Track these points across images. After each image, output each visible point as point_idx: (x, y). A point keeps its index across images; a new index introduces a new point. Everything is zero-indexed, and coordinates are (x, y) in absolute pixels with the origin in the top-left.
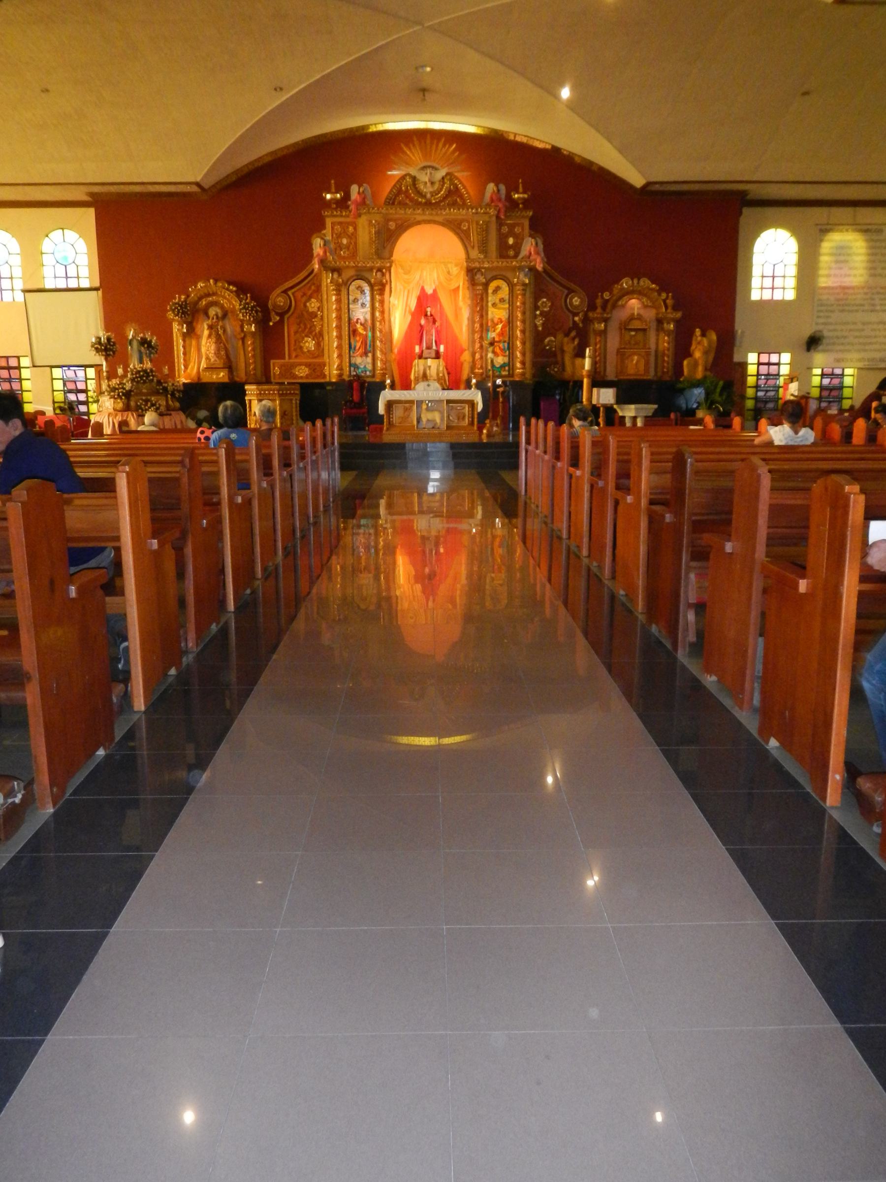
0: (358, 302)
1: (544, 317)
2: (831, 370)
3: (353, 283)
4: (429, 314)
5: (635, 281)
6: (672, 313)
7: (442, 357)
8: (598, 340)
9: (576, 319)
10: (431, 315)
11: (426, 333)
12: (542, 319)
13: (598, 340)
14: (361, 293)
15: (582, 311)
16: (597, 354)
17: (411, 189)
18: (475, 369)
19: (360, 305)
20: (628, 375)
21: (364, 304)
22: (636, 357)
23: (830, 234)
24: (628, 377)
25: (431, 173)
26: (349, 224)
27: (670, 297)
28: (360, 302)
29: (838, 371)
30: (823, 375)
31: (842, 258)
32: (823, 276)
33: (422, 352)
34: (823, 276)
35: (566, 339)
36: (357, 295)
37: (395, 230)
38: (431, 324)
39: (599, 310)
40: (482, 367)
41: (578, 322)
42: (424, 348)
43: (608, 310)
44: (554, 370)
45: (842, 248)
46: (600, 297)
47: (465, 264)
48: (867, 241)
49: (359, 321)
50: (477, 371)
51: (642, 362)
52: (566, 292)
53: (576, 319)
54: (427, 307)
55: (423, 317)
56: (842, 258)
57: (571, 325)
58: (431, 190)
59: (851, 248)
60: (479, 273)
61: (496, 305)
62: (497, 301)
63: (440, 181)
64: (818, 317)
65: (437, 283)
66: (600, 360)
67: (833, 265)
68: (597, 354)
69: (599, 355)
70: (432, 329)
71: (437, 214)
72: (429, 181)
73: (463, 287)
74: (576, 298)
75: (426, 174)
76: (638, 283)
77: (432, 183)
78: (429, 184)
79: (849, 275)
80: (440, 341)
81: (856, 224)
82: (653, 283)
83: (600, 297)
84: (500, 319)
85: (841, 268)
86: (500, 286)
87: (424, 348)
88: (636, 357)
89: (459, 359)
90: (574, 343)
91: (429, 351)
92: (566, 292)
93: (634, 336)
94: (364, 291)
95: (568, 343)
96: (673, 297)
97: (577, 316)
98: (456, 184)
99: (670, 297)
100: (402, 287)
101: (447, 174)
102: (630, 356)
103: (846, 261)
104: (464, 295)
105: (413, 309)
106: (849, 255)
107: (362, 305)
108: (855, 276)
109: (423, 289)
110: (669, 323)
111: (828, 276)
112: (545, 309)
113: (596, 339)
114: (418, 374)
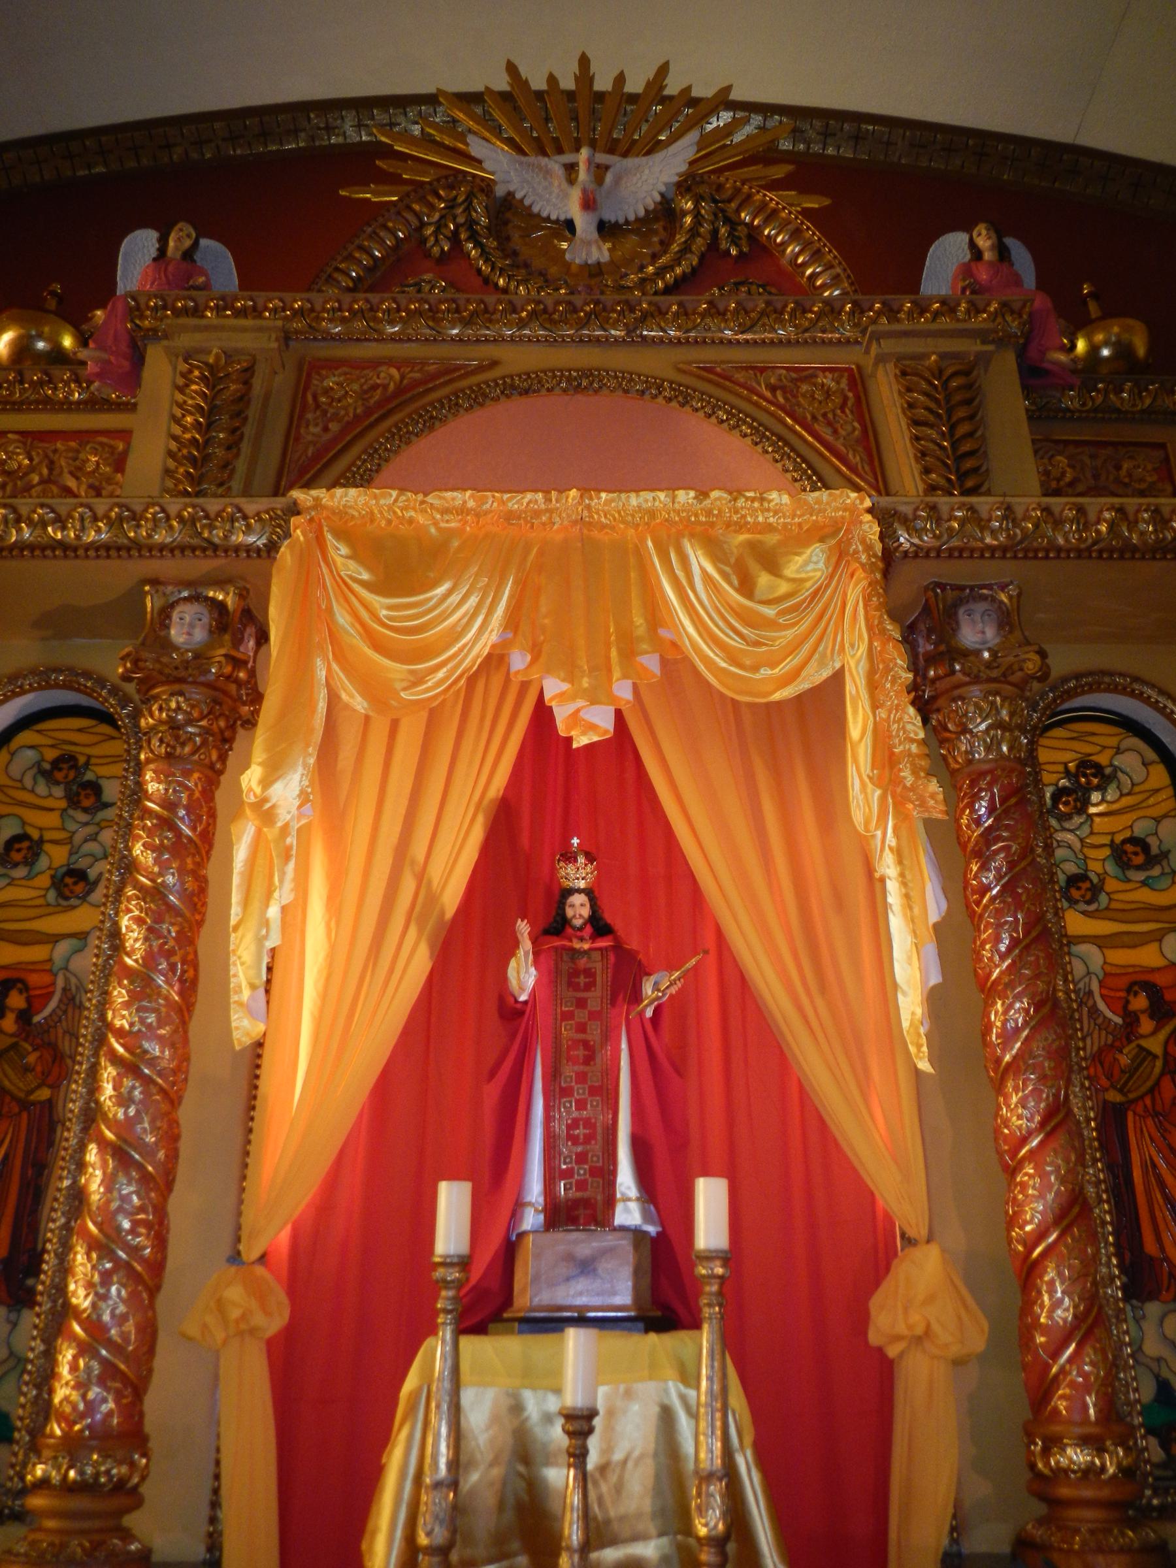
0: (31, 860)
3: (26, 737)
4: (578, 908)
7: (710, 1311)
10: (598, 926)
11: (552, 1076)
14: (73, 801)
17: (478, 244)
18: (1053, 1443)
19: (44, 880)
21: (80, 875)
25: (600, 171)
26: (83, 436)
28: (57, 856)
33: (510, 1250)
36: (31, 816)
37: (357, 419)
38: (595, 998)
40: (1110, 1411)
42: (531, 1220)
47: (871, 529)
49: (16, 1000)
50: (1076, 1456)
54: (570, 857)
55: (523, 928)
58: (600, 253)
60: (981, 607)
61: (1096, 890)
62: (1099, 863)
63: (649, 218)
65: (651, 662)
70: (610, 1036)
71: (634, 341)
72: (588, 204)
73: (873, 686)
75: (571, 168)
77: (605, 229)
78: (584, 223)
80: (679, 1144)
84: (1132, 988)
86: (1103, 759)
87: (531, 1220)
89: (861, 1320)
91: (582, 1243)
94: (95, 788)
98: (750, 226)
100: (359, 703)
101: (687, 184)
104: (881, 738)
105: (451, 897)
107: (58, 883)
109: (543, 715)
114: (457, 1511)
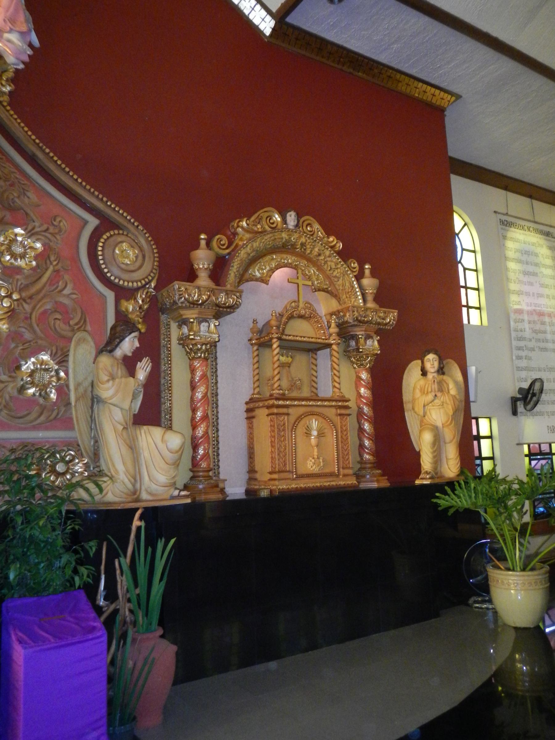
1: (20, 291)
2: (537, 446)
5: (291, 218)
6: (376, 311)
8: (199, 374)
9: (129, 306)
12: (9, 296)
13: (199, 374)
15: (144, 286)
16: (199, 414)
20: (302, 476)
22: (315, 424)
23: (512, 229)
24: (303, 484)
27: (367, 272)
29: (545, 448)
30: (531, 455)
31: (531, 269)
32: (514, 292)
34: (514, 292)
35: (105, 360)
39: (203, 280)
41: (132, 317)
43: (228, 287)
44: (53, 471)
45: (527, 253)
46: (203, 243)
48: (550, 248)
51: (331, 439)
52: (93, 222)
53: (129, 306)
56: (531, 269)
57: (111, 320)
59: (536, 255)
64: (519, 358)
66: (206, 433)
67: (521, 277)
68: (199, 414)
69: (205, 417)
74: (125, 246)
76: (297, 226)
79: (540, 296)
81: (535, 222)
82: (328, 234)
83: (203, 243)
85: (531, 284)
88: (315, 424)
90: (132, 373)
92: (93, 222)
93: (289, 365)
95: (112, 378)
96: (373, 274)
97: (128, 300)
99: (367, 272)
102: (299, 418)
103: (535, 274)
106: (536, 265)
108: (548, 297)
110: (368, 337)
111: (519, 293)
112: (20, 263)
113: (193, 371)
